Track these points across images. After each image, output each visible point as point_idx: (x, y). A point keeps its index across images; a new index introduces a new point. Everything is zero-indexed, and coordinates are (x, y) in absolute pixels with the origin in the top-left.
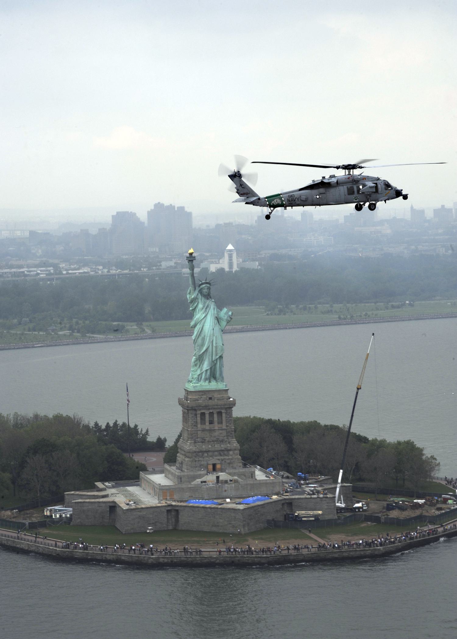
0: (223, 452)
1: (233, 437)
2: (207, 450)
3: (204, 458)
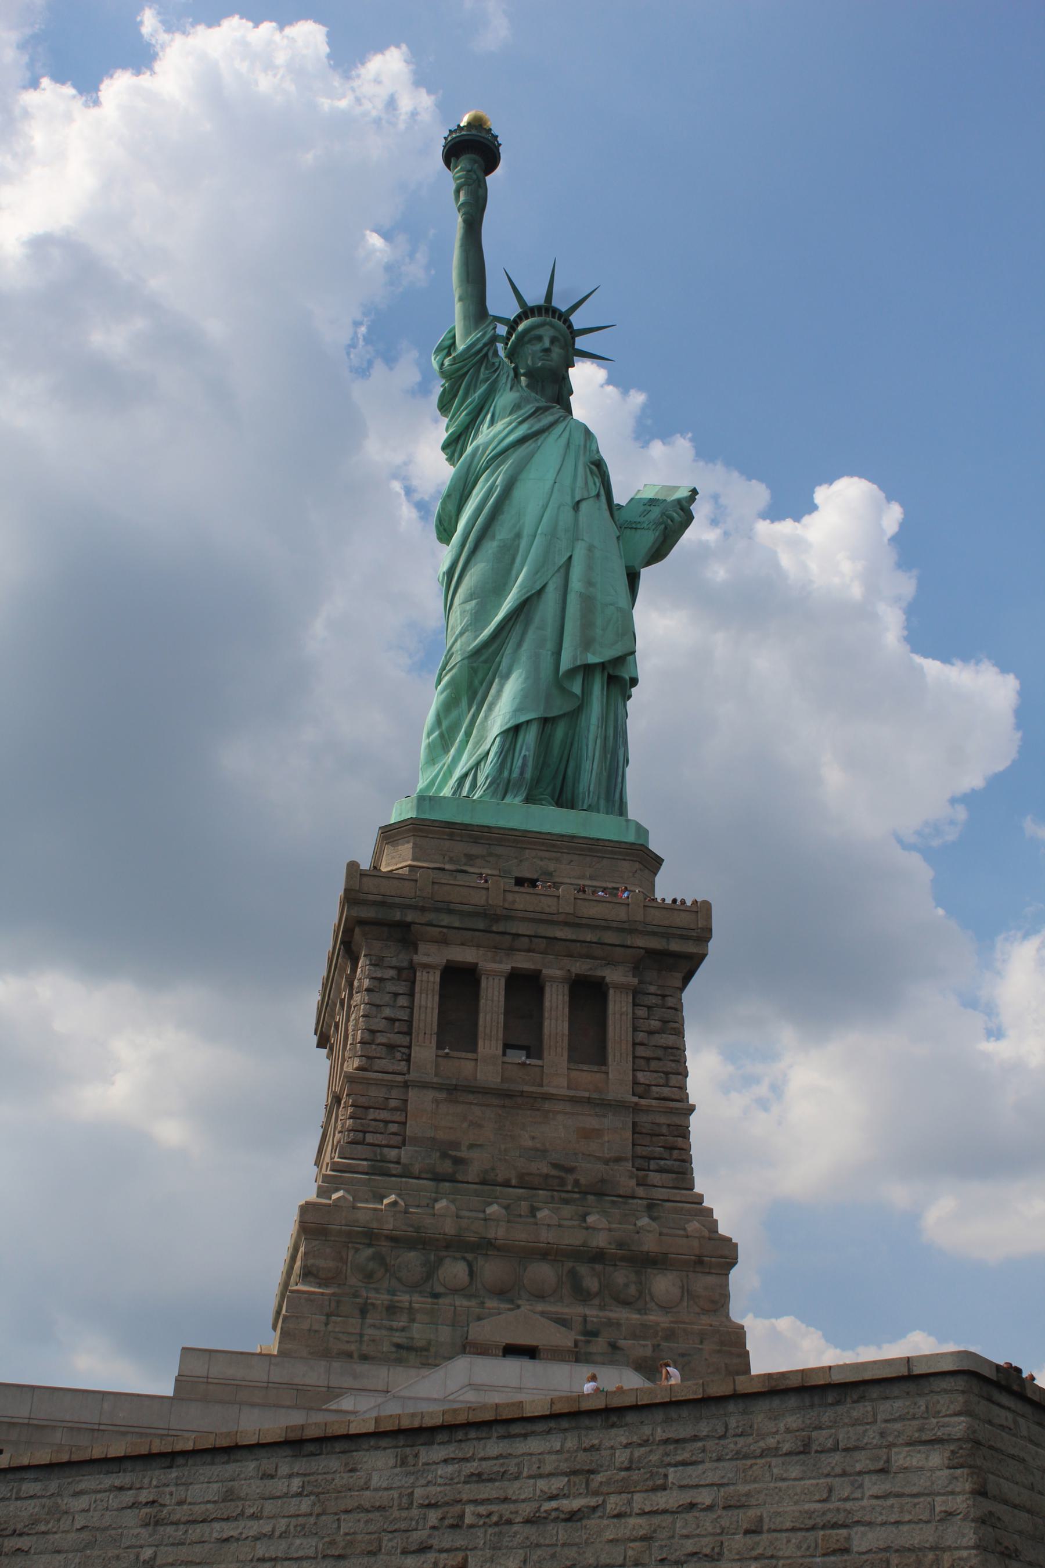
0: (598, 1267)
2: (472, 1238)
3: (436, 1296)
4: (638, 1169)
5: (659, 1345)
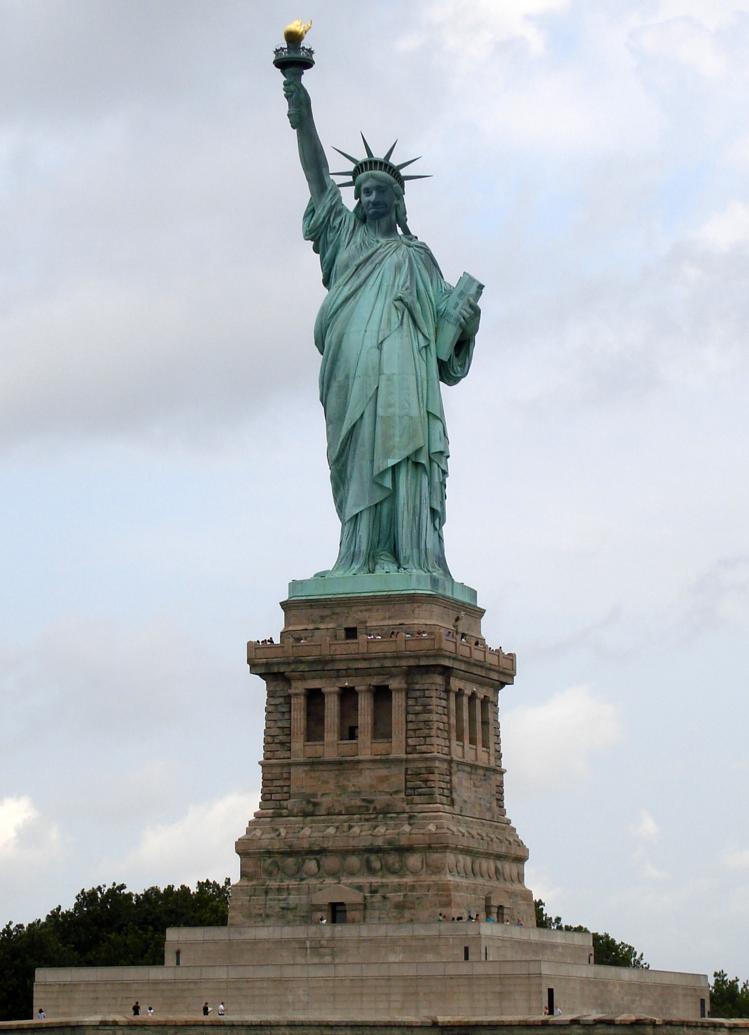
1: (432, 794)
2: (316, 848)
3: (302, 880)
4: (408, 796)
5: (406, 895)
